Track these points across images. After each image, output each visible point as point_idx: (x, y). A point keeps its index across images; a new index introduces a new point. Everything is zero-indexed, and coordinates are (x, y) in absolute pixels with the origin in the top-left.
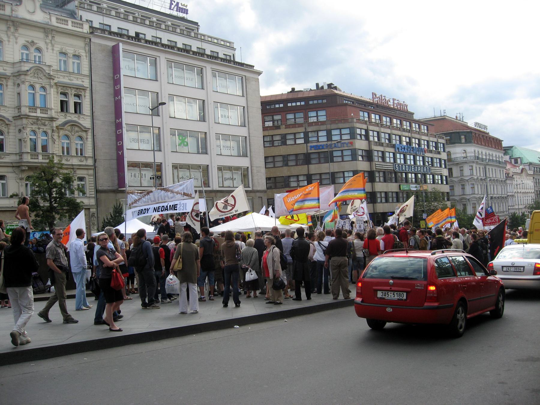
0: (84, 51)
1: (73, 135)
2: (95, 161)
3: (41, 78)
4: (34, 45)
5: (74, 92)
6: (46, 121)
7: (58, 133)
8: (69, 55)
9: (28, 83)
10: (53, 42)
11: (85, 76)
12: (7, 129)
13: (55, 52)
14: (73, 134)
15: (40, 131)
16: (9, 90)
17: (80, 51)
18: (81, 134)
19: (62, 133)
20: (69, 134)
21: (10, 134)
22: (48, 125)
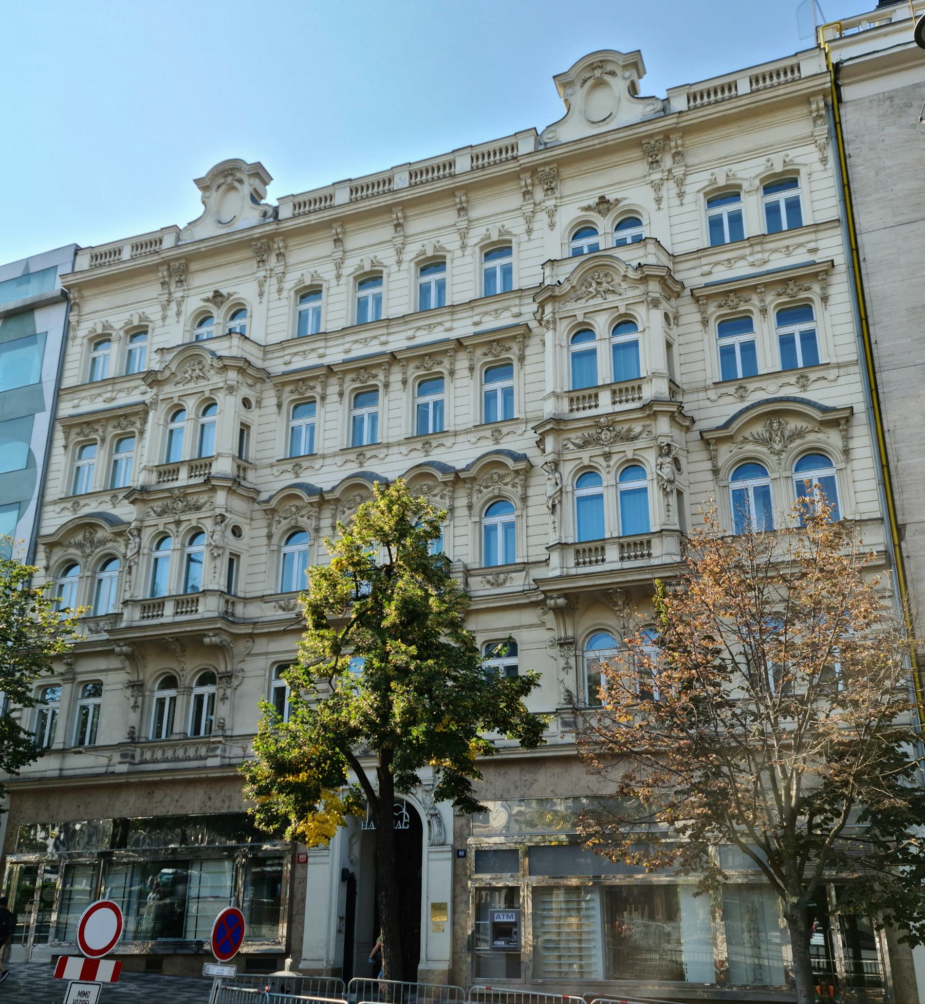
0: (812, 148)
1: (779, 453)
2: (898, 531)
3: (613, 292)
4: (608, 210)
5: (772, 300)
6: (634, 425)
7: (713, 458)
8: (745, 186)
9: (565, 322)
10: (678, 171)
11: (817, 227)
12: (519, 489)
13: (687, 199)
14: (778, 447)
15: (612, 463)
16: (528, 369)
17: (792, 153)
18: (813, 439)
19: (726, 454)
20: (760, 451)
21: (531, 502)
22: (644, 436)
